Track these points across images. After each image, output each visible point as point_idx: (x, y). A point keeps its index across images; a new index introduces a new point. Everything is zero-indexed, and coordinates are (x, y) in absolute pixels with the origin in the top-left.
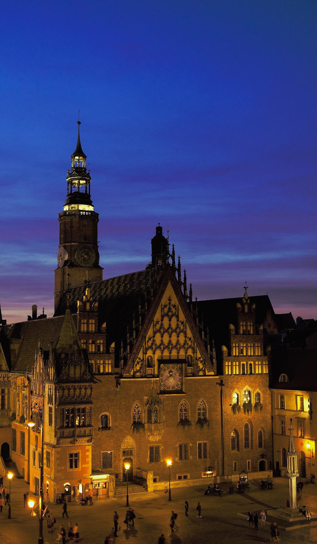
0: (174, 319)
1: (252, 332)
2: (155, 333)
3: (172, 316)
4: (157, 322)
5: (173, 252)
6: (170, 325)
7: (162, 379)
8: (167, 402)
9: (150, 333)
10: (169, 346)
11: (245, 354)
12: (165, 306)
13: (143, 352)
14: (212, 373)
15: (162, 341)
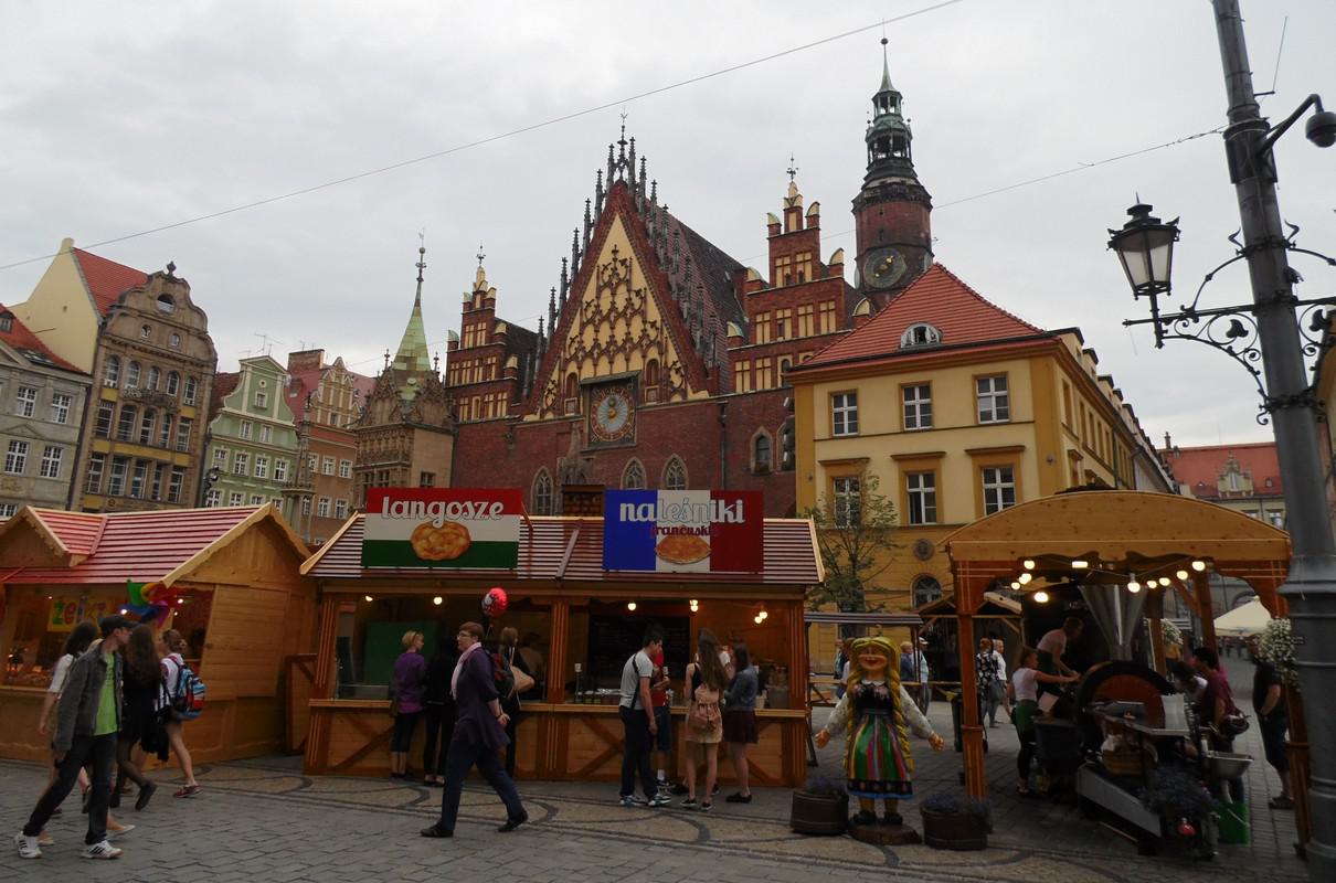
0: (622, 289)
1: (808, 278)
2: (583, 326)
3: (618, 284)
4: (589, 304)
5: (632, 153)
6: (613, 303)
7: (594, 419)
8: (599, 467)
9: (574, 331)
10: (610, 350)
11: (788, 336)
12: (606, 267)
13: (559, 369)
14: (704, 395)
15: (596, 340)
